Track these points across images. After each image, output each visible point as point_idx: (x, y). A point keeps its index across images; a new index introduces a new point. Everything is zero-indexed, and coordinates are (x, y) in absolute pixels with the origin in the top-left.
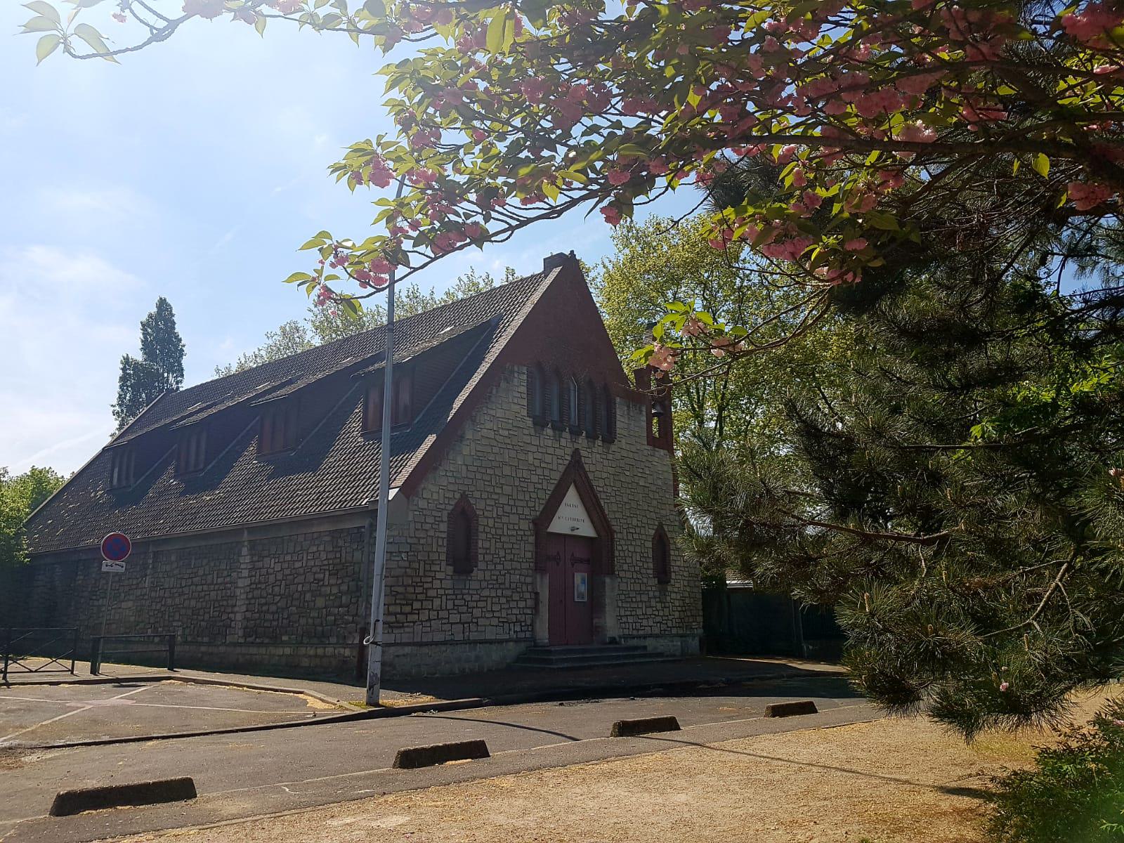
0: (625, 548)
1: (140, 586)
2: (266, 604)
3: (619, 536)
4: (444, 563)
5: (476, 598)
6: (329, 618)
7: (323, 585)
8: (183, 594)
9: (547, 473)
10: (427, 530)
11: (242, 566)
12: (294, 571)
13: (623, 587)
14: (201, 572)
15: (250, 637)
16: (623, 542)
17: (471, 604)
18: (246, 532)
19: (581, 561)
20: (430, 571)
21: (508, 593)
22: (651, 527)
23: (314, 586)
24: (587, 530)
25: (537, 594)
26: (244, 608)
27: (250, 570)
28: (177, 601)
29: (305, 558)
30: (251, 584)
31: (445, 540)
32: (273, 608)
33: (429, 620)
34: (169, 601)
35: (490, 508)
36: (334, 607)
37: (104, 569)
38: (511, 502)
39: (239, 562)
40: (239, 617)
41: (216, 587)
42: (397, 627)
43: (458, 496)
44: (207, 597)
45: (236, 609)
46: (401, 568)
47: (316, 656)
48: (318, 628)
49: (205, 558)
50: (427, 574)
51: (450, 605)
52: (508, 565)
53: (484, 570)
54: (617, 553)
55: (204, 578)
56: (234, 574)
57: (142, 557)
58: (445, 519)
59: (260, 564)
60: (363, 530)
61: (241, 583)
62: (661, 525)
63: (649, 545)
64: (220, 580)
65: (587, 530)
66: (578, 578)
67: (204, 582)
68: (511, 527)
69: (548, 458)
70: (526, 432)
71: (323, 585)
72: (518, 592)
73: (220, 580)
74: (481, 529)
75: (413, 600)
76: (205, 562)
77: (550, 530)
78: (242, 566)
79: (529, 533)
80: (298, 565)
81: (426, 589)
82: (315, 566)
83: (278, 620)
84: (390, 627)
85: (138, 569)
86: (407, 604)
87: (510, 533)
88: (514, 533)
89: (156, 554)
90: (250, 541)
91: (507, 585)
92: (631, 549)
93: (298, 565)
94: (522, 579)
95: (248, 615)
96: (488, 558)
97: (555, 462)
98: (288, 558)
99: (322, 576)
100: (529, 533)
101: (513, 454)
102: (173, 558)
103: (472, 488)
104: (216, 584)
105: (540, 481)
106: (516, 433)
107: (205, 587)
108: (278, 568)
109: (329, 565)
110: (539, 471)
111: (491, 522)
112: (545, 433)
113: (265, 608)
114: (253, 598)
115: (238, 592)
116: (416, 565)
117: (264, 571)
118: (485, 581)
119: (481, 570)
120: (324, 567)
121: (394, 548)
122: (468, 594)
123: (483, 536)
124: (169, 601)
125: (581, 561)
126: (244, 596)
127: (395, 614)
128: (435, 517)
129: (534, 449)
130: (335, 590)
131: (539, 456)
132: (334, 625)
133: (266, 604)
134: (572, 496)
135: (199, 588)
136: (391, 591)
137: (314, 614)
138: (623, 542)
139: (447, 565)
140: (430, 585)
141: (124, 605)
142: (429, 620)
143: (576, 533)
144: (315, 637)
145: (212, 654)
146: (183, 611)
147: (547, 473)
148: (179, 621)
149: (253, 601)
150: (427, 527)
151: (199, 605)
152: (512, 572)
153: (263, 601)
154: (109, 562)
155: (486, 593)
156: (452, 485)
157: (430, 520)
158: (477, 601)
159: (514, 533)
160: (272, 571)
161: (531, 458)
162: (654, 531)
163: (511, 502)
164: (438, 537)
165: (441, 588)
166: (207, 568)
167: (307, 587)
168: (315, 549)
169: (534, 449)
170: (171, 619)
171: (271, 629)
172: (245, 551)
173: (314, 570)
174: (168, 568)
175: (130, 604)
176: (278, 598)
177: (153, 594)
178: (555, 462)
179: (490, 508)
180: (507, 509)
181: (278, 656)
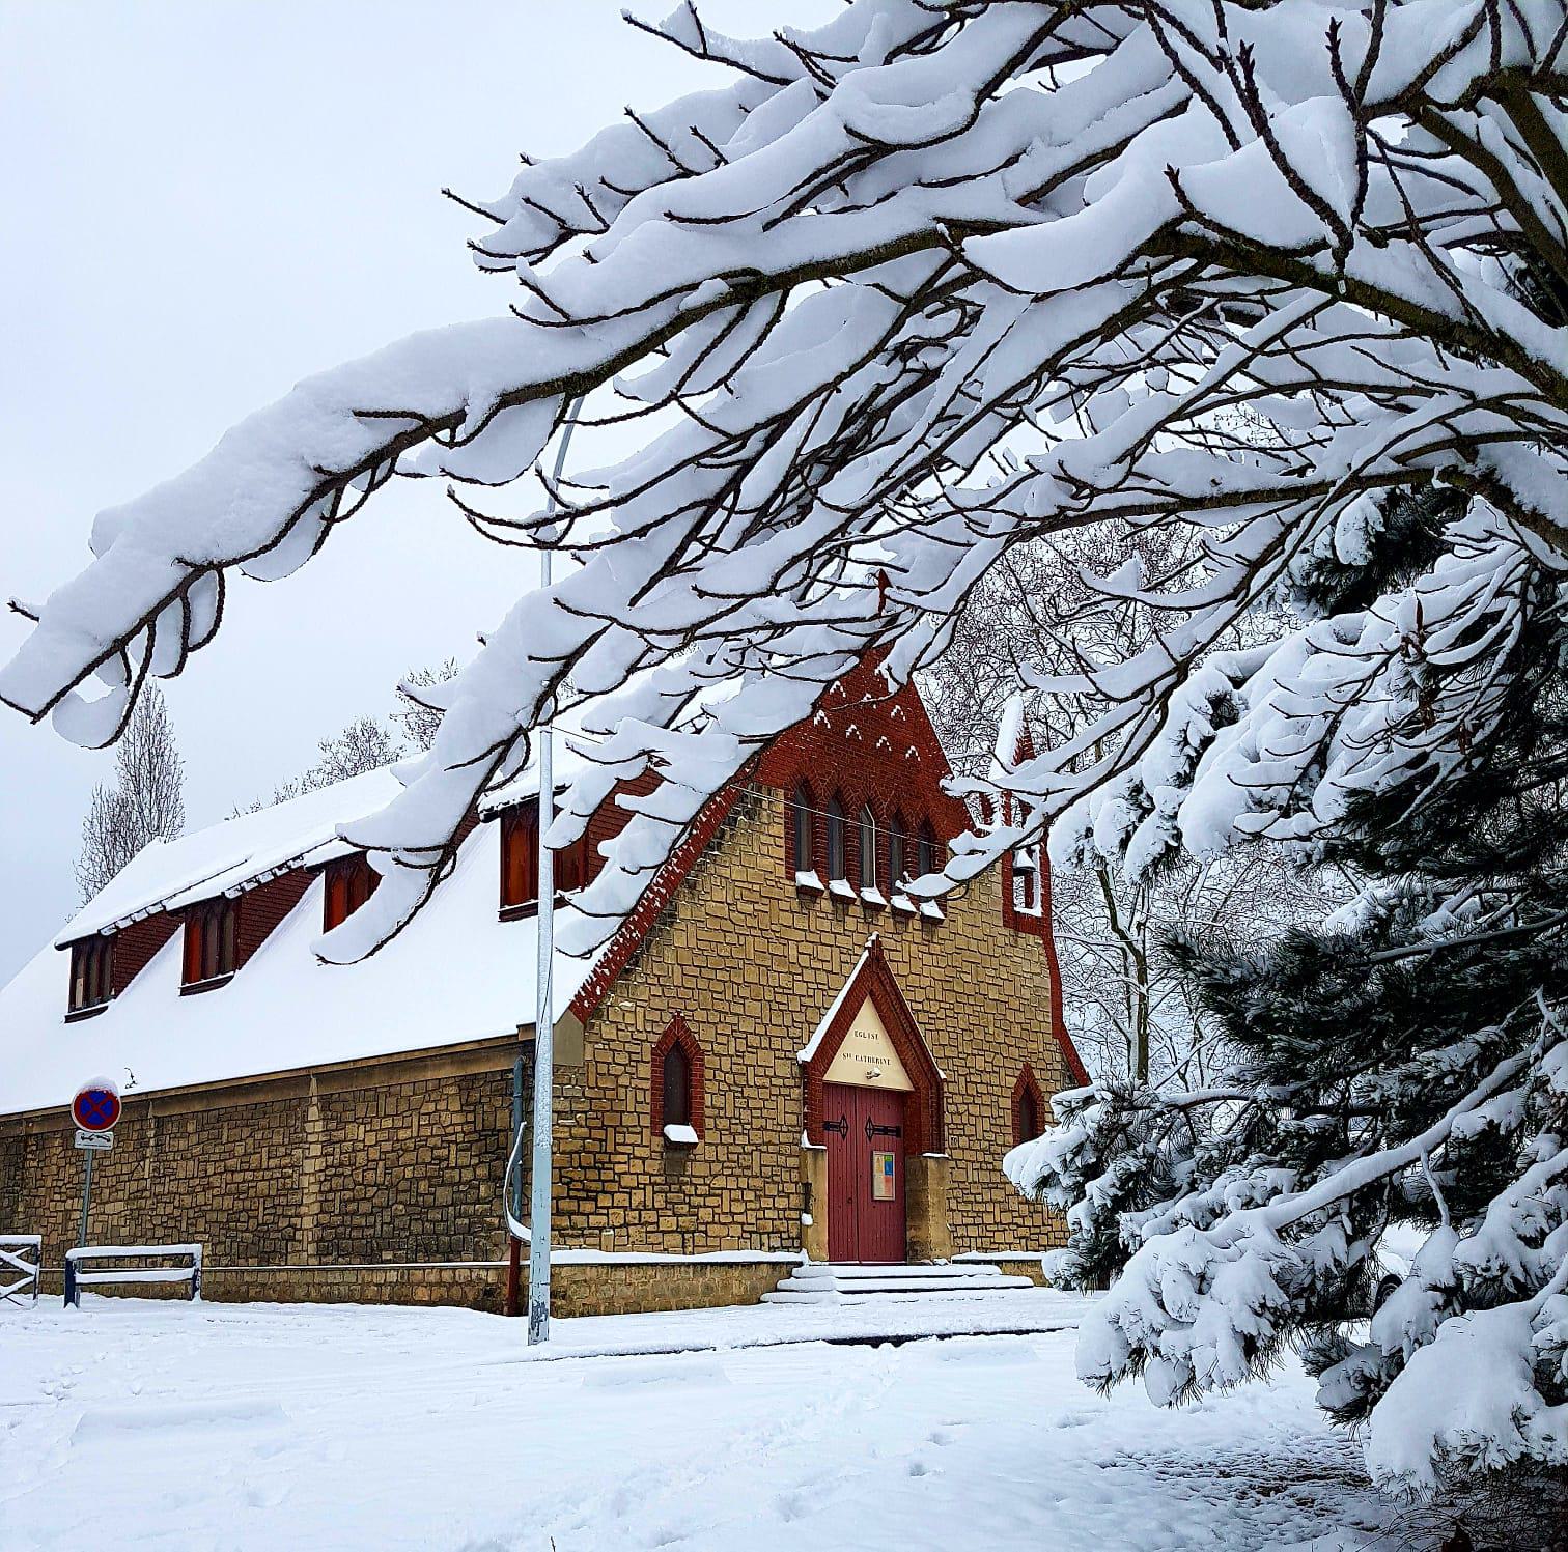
0: (962, 1108)
1: (135, 1176)
2: (353, 1200)
3: (952, 1087)
4: (646, 1132)
5: (702, 1190)
6: (459, 1221)
7: (447, 1168)
8: (209, 1187)
9: (822, 977)
10: (617, 1077)
11: (311, 1138)
12: (398, 1146)
13: (959, 1175)
14: (240, 1150)
15: (328, 1254)
16: (957, 1099)
17: (696, 1201)
18: (314, 1081)
19: (885, 1131)
20: (624, 1144)
21: (758, 1183)
22: (1009, 1072)
23: (432, 1170)
24: (894, 1077)
25: (807, 1186)
26: (316, 1208)
27: (324, 1144)
28: (201, 1199)
29: (415, 1123)
30: (327, 1167)
31: (648, 1093)
32: (365, 1207)
33: (626, 1225)
34: (187, 1200)
35: (723, 1040)
36: (466, 1203)
37: (79, 1143)
38: (760, 1030)
39: (303, 1130)
40: (308, 1222)
41: (268, 1174)
42: (573, 1236)
43: (668, 1018)
44: (252, 1192)
45: (303, 1210)
46: (574, 1138)
47: (440, 1284)
48: (442, 1238)
49: (247, 1126)
50: (620, 1149)
51: (660, 1202)
52: (756, 1137)
53: (716, 1145)
54: (947, 1118)
55: (245, 1159)
56: (298, 1152)
57: (137, 1126)
58: (648, 1058)
59: (341, 1135)
60: (511, 1076)
61: (309, 1166)
62: (1028, 1068)
63: (1007, 1103)
64: (273, 1163)
65: (894, 1077)
66: (880, 1160)
67: (245, 1166)
68: (761, 1071)
69: (825, 952)
70: (784, 906)
71: (447, 1168)
72: (774, 1182)
73: (273, 1163)
74: (709, 1074)
75: (598, 1192)
76: (246, 1132)
77: (826, 1078)
78: (311, 1138)
79: (792, 1082)
80: (402, 1135)
81: (619, 1174)
82: (432, 1136)
83: (374, 1226)
84: (562, 1235)
85: (131, 1149)
86: (588, 1198)
87: (759, 1082)
88: (767, 1082)
89: (160, 1123)
90: (321, 1097)
91: (756, 1170)
92: (974, 1110)
93: (402, 1135)
94: (781, 1160)
95: (324, 1219)
96: (723, 1123)
97: (836, 961)
98: (388, 1123)
99: (446, 1151)
100: (792, 1082)
101: (761, 944)
102: (191, 1128)
103: (692, 1005)
104: (267, 1169)
105: (811, 993)
106: (766, 909)
107: (249, 1175)
108: (371, 1139)
109: (455, 1133)
110: (809, 975)
111: (726, 1064)
112: (818, 907)
113: (352, 1207)
114: (330, 1190)
115: (305, 1182)
116: (600, 1134)
117: (347, 1146)
118: (718, 1161)
119: (710, 1144)
120: (449, 1138)
121: (564, 1105)
122: (691, 1184)
123: (711, 1087)
124: (187, 1200)
125: (885, 1131)
126: (315, 1188)
127: (571, 1214)
128: (630, 1053)
129: (800, 936)
130: (468, 1175)
131: (807, 948)
132: (469, 1233)
133: (353, 1200)
134: (867, 1018)
135: (238, 1177)
136: (561, 1176)
137: (435, 1215)
138: (957, 1099)
139: (652, 1134)
140: (624, 1168)
141: (109, 1208)
142: (626, 1225)
143: (875, 1083)
144: (437, 1252)
145: (263, 1285)
146: (212, 1216)
147: (822, 977)
148: (205, 1232)
149: (331, 1196)
150: (616, 1070)
151: (239, 1205)
152: (764, 1148)
153: (349, 1195)
154: (89, 1133)
155: (719, 1182)
156: (657, 1000)
157: (622, 1058)
158: (705, 1196)
159: (767, 1082)
160: (361, 1146)
161: (793, 952)
162: (1015, 1080)
163: (760, 1030)
164: (636, 1088)
165: (645, 1173)
166: (250, 1141)
167: (420, 1172)
168: (431, 1107)
169: (800, 936)
170: (191, 1230)
171: (364, 1242)
172: (314, 1113)
173: (432, 1142)
174: (183, 1144)
175: (120, 1206)
176: (372, 1191)
177: (159, 1189)
178: (836, 961)
179: (723, 1040)
180: (753, 1040)
181: (377, 1285)
